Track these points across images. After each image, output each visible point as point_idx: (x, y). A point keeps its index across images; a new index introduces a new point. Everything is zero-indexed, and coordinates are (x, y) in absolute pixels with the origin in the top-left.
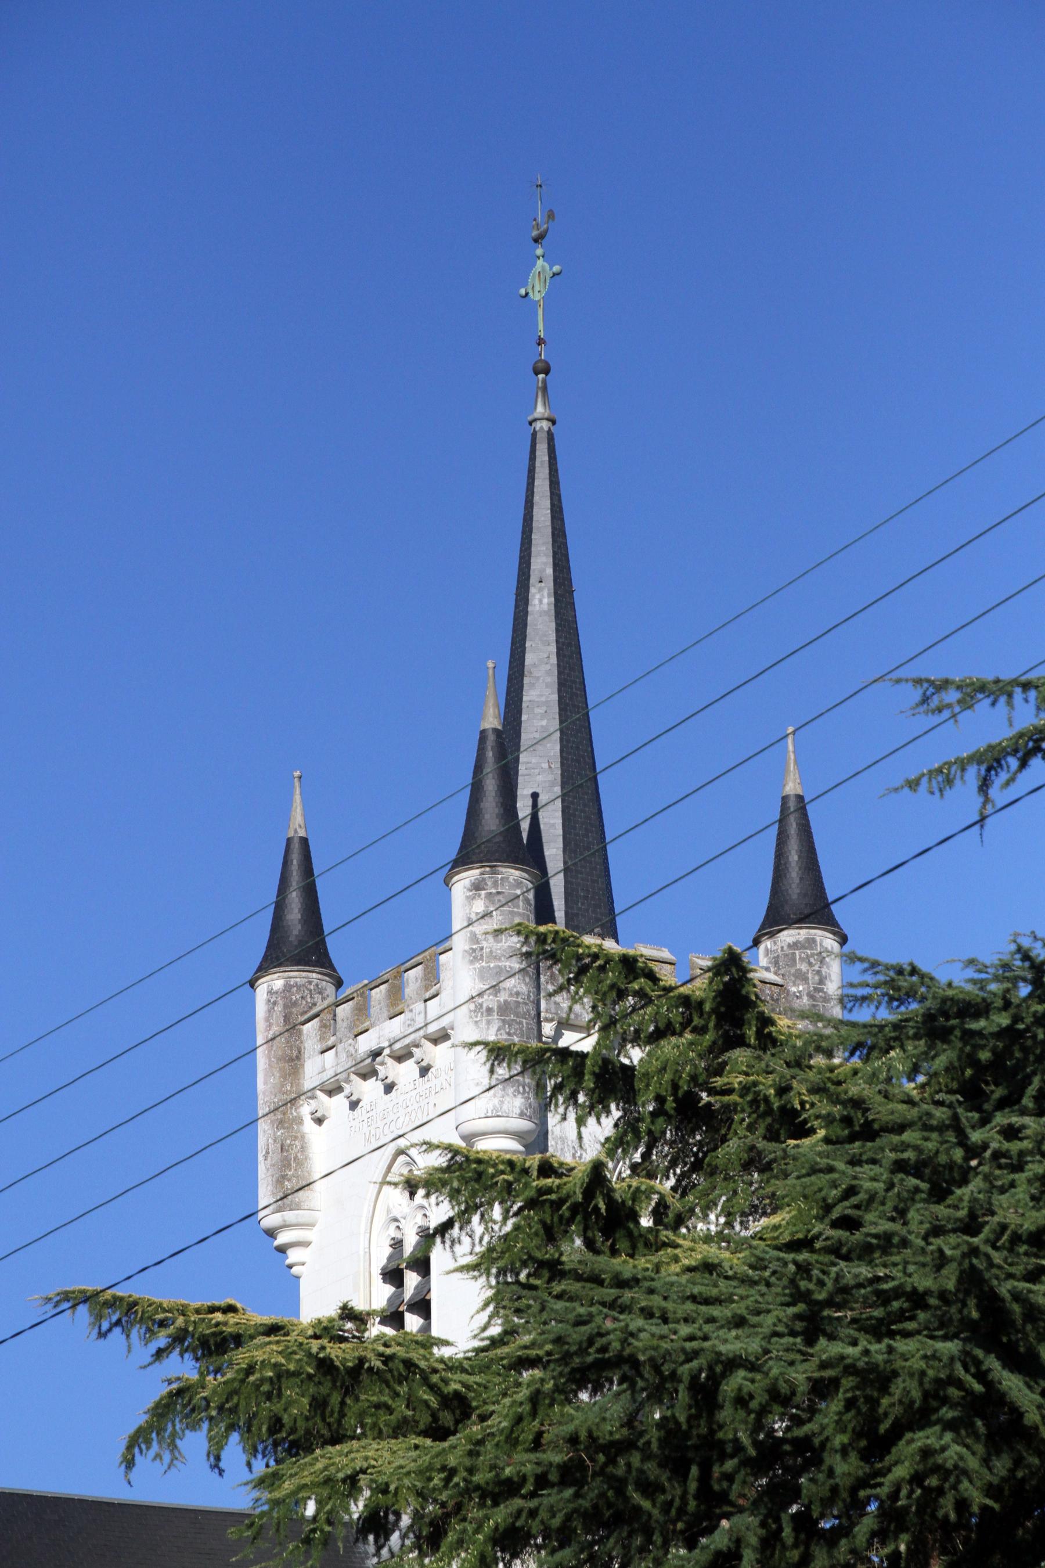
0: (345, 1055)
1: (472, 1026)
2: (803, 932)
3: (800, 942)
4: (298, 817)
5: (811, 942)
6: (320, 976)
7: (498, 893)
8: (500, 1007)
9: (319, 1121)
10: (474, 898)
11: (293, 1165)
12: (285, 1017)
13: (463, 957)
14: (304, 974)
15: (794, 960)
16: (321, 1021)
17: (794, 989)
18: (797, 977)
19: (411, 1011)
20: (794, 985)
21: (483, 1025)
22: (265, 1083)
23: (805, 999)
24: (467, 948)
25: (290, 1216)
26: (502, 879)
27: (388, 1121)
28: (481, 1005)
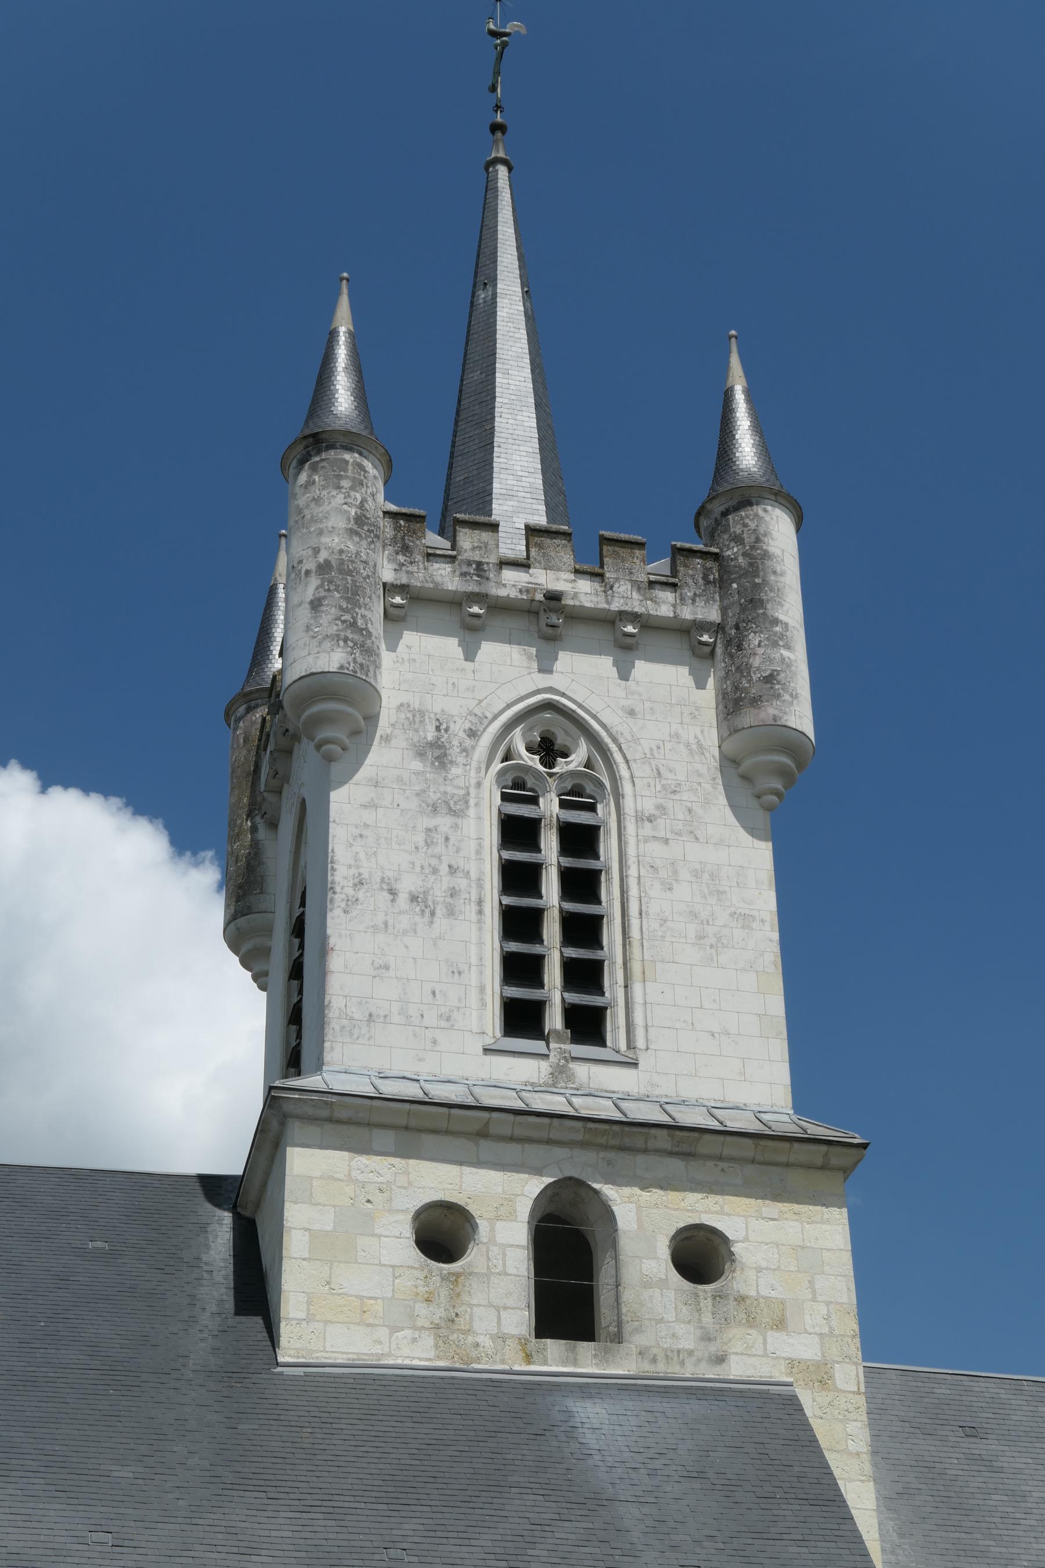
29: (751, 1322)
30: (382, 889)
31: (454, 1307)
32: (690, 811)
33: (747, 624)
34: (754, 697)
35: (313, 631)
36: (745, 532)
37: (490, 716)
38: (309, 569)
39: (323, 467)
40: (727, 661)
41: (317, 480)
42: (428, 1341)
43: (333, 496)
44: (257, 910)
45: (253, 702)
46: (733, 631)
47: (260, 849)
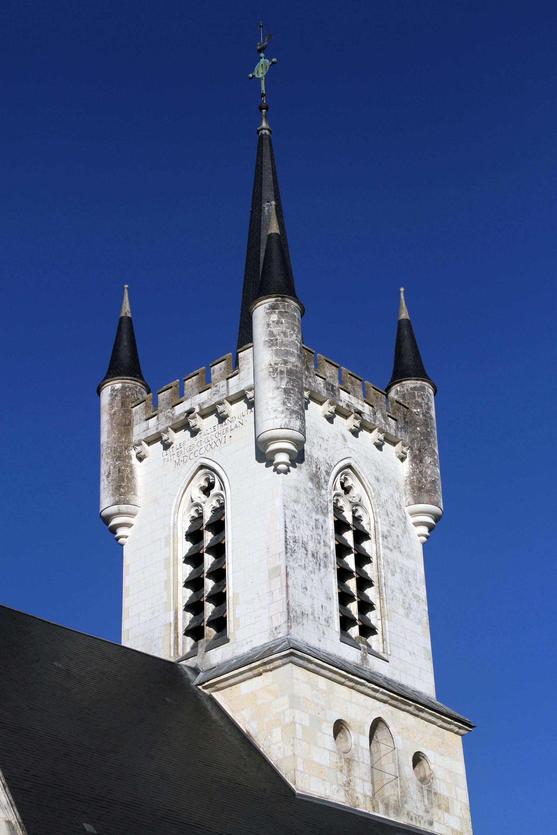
0: (164, 418)
1: (271, 380)
2: (419, 382)
3: (417, 387)
4: (126, 310)
5: (423, 388)
6: (141, 385)
7: (286, 312)
8: (288, 371)
9: (140, 459)
10: (271, 313)
11: (126, 480)
12: (122, 403)
13: (264, 344)
14: (133, 382)
15: (415, 396)
16: (146, 404)
17: (415, 410)
18: (416, 405)
19: (216, 386)
20: (415, 408)
21: (278, 379)
22: (109, 437)
23: (421, 416)
24: (267, 339)
25: (123, 508)
26: (287, 305)
27: (193, 451)
28: (277, 369)
29: (439, 806)
30: (303, 547)
31: (349, 777)
32: (398, 536)
33: (425, 451)
34: (429, 490)
35: (287, 405)
36: (423, 403)
37: (333, 467)
38: (282, 370)
39: (286, 316)
40: (414, 465)
41: (284, 322)
42: (342, 793)
43: (291, 334)
44: (133, 504)
45: (127, 384)
46: (417, 452)
47: (133, 470)
